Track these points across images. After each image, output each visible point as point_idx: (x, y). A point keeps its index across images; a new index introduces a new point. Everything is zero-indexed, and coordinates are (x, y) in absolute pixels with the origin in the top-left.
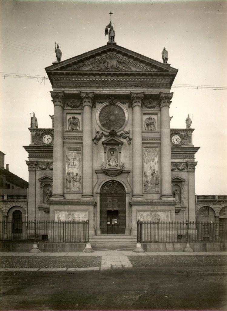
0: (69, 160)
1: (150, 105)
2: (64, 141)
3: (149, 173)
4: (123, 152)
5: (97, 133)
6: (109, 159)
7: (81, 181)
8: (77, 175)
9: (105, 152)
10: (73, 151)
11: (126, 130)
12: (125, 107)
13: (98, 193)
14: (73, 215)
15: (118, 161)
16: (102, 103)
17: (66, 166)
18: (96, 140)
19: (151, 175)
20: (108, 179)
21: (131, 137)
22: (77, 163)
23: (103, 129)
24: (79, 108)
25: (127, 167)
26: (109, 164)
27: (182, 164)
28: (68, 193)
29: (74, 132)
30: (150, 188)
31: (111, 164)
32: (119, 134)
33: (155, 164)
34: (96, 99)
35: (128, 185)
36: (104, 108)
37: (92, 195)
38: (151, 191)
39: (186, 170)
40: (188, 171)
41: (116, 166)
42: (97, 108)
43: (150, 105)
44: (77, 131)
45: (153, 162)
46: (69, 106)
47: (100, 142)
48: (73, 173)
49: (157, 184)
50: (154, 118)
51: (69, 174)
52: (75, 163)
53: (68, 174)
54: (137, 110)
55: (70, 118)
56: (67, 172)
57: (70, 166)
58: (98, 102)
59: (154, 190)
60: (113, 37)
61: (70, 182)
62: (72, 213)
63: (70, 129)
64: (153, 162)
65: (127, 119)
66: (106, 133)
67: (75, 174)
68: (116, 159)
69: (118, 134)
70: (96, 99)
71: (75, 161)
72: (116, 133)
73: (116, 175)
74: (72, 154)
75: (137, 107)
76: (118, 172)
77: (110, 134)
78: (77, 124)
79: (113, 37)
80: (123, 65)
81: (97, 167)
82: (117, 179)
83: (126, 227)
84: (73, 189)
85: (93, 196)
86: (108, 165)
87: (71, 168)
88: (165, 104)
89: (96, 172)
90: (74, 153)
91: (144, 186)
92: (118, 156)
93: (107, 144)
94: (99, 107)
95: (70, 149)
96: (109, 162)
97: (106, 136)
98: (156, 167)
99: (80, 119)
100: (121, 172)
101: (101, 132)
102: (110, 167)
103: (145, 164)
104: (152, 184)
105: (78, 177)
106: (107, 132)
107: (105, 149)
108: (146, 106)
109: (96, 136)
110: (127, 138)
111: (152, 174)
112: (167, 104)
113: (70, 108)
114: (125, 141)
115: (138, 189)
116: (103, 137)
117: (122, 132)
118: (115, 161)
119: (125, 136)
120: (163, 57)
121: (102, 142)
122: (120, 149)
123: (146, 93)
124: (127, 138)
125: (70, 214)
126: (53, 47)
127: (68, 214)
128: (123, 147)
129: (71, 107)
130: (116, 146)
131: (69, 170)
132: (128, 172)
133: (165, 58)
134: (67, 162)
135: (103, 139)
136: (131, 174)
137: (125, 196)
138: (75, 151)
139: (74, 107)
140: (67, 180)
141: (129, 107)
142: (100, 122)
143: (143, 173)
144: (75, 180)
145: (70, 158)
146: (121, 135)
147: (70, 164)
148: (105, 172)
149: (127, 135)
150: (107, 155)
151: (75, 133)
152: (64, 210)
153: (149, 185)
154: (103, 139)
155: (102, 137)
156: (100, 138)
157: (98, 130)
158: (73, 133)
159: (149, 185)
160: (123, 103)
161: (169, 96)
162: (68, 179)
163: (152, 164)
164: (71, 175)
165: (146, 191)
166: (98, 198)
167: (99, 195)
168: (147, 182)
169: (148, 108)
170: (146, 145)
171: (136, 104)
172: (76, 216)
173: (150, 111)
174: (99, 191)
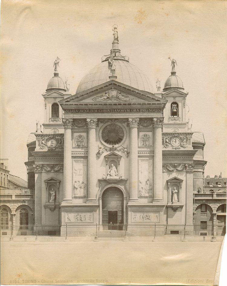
1: (145, 125)
9: (107, 164)
10: (79, 164)
18: (98, 154)
24: (85, 128)
27: (181, 165)
28: (75, 198)
39: (184, 170)
40: (186, 172)
42: (99, 127)
43: (145, 125)
47: (102, 157)
86: (109, 175)
102: (112, 178)
108: (142, 125)
109: (99, 151)
115: (135, 195)
121: (104, 156)
123: (142, 117)
135: (106, 153)
136: (128, 182)
140: (74, 187)
143: (139, 181)
164: (77, 182)
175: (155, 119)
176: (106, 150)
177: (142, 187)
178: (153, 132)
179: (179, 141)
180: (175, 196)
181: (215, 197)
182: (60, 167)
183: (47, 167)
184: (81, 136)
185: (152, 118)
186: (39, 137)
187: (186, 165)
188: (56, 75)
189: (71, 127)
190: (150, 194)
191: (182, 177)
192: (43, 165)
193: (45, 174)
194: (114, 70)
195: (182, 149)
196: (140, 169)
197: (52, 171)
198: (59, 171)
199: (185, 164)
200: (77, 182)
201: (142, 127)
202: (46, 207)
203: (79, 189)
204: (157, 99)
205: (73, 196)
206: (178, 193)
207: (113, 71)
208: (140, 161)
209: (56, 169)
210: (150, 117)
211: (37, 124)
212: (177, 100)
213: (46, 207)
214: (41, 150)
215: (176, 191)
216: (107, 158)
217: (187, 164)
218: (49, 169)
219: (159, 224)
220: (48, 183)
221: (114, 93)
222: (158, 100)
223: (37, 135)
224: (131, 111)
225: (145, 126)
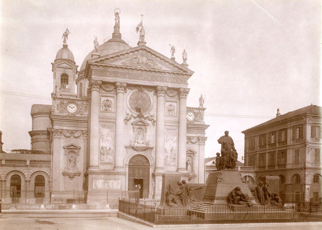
0: (103, 136)
1: (171, 95)
3: (169, 151)
4: (148, 130)
5: (128, 114)
6: (137, 137)
7: (113, 154)
8: (110, 149)
10: (106, 129)
11: (152, 114)
12: (151, 94)
14: (108, 183)
16: (132, 90)
17: (101, 141)
18: (127, 120)
19: (170, 151)
20: (136, 153)
21: (155, 119)
22: (110, 139)
23: (133, 111)
25: (152, 145)
28: (102, 164)
29: (107, 112)
30: (169, 162)
31: (139, 141)
32: (145, 116)
33: (174, 142)
34: (129, 86)
35: (152, 158)
36: (134, 93)
38: (170, 164)
42: (127, 94)
43: (171, 95)
44: (110, 112)
45: (172, 140)
46: (104, 90)
48: (106, 148)
50: (174, 106)
51: (102, 148)
52: (108, 139)
53: (102, 148)
54: (161, 99)
55: (105, 100)
56: (101, 147)
57: (104, 141)
58: (128, 88)
59: (173, 163)
60: (143, 36)
61: (104, 155)
62: (107, 181)
63: (104, 109)
64: (172, 140)
65: (152, 104)
66: (135, 115)
67: (108, 148)
68: (143, 137)
69: (145, 116)
70: (129, 86)
71: (108, 138)
72: (143, 116)
73: (143, 151)
74: (105, 131)
75: (161, 97)
77: (138, 116)
78: (111, 107)
79: (143, 36)
80: (151, 61)
81: (128, 144)
83: (149, 193)
84: (106, 161)
86: (136, 143)
87: (105, 143)
88: (183, 96)
89: (126, 148)
90: (107, 130)
92: (145, 134)
93: (136, 125)
94: (130, 92)
95: (104, 126)
97: (135, 118)
98: (175, 145)
99: (113, 101)
100: (146, 149)
101: (130, 114)
102: (139, 145)
103: (166, 142)
104: (171, 159)
105: (110, 151)
106: (136, 114)
107: (134, 128)
110: (152, 120)
111: (171, 151)
112: (186, 96)
113: (104, 92)
114: (149, 122)
116: (132, 118)
117: (148, 115)
119: (150, 118)
120: (183, 57)
122: (146, 129)
124: (152, 120)
125: (106, 182)
126: (94, 39)
127: (104, 183)
128: (148, 127)
129: (106, 91)
130: (143, 127)
131: (104, 144)
132: (152, 148)
134: (101, 138)
135: (133, 120)
137: (149, 168)
138: (108, 129)
139: (108, 91)
140: (101, 153)
141: (154, 95)
142: (130, 105)
144: (108, 153)
145: (104, 134)
146: (147, 117)
147: (104, 140)
148: (133, 148)
149: (152, 118)
150: (135, 133)
151: (108, 114)
152: (101, 179)
153: (169, 159)
154: (133, 120)
155: (131, 118)
156: (130, 119)
157: (128, 112)
158: (106, 114)
159: (169, 159)
160: (149, 91)
161: (187, 90)
162: (103, 152)
163: (171, 142)
165: (166, 164)
166: (127, 169)
167: (128, 166)
168: (167, 157)
169: (169, 97)
170: (166, 127)
171: (161, 94)
172: (110, 184)
173: (171, 99)
174: (128, 163)
176: (134, 117)
178: (178, 102)
181: (276, 168)
182: (80, 134)
183: (67, 133)
184: (109, 101)
188: (65, 47)
193: (64, 139)
195: (196, 123)
197: (72, 137)
198: (79, 138)
201: (168, 97)
202: (64, 174)
204: (184, 70)
205: (100, 162)
209: (76, 135)
210: (177, 87)
213: (64, 174)
214: (61, 114)
218: (68, 135)
220: (67, 148)
222: (185, 71)
225: (171, 97)
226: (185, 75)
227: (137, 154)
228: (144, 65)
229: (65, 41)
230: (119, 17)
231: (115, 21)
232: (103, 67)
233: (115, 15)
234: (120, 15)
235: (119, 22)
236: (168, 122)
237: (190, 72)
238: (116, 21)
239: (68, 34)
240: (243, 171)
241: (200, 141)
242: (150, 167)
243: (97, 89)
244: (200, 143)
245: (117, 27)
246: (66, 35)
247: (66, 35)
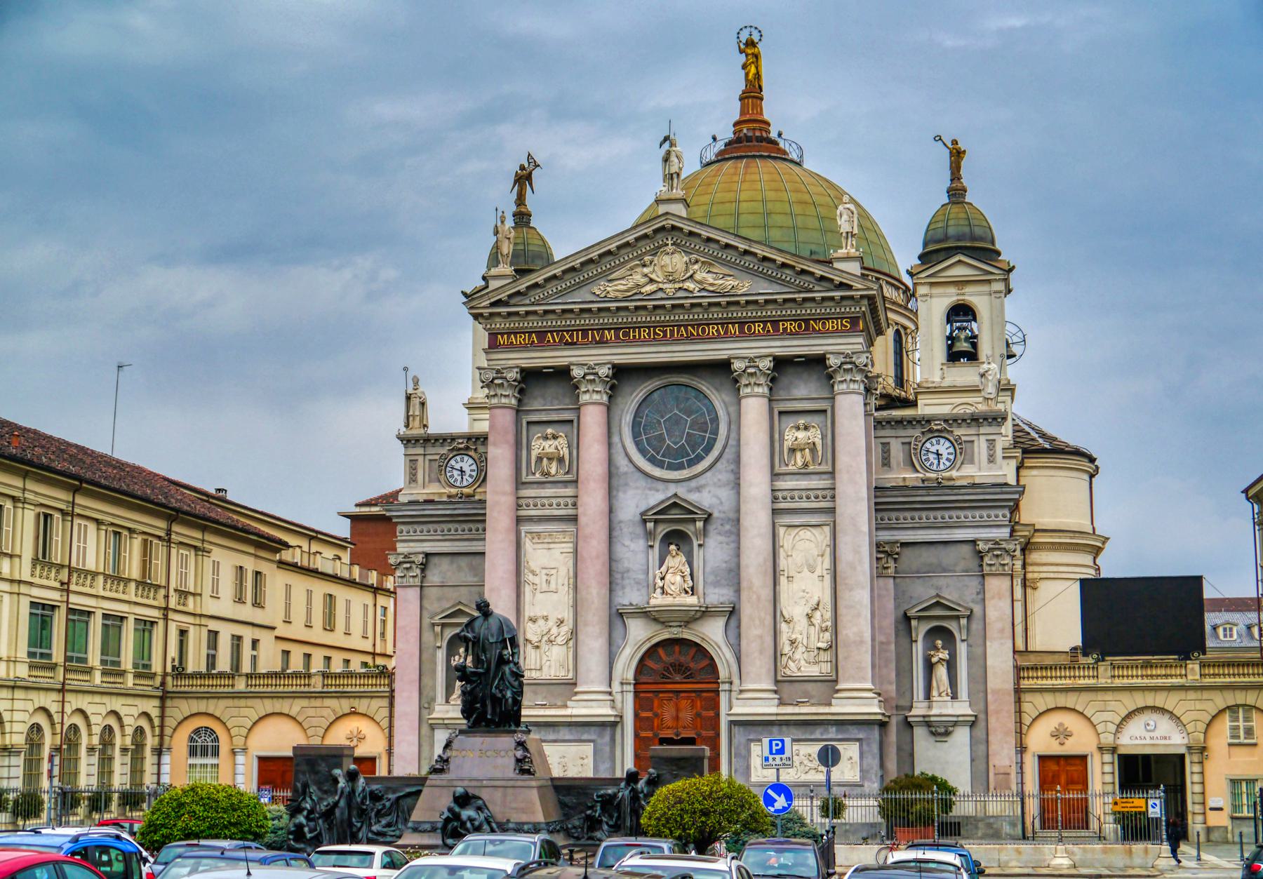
2: (522, 513)
13: (627, 684)
15: (692, 575)
19: (805, 621)
26: (663, 588)
37: (609, 690)
41: (687, 592)
49: (825, 650)
61: (537, 647)
75: (754, 399)
76: (693, 613)
82: (686, 634)
85: (610, 694)
91: (782, 655)
96: (662, 579)
102: (668, 600)
111: (809, 617)
118: (683, 577)
133: (847, 233)
137: (717, 692)
147: (538, 587)
159: (801, 649)
164: (541, 622)
165: (789, 673)
166: (630, 698)
167: (631, 688)
174: (630, 676)
175: (833, 361)
177: (794, 637)
179: (951, 450)
180: (941, 672)
185: (824, 355)
186: (414, 446)
187: (981, 546)
189: (514, 402)
190: (826, 668)
191: (956, 591)
192: (427, 555)
194: (675, 176)
196: (782, 563)
199: (974, 542)
200: (541, 622)
203: (544, 647)
204: (837, 279)
206: (951, 665)
207: (672, 179)
208: (782, 531)
211: (408, 398)
212: (977, 298)
215: (944, 655)
216: (650, 521)
217: (987, 541)
219: (858, 790)
221: (674, 261)
222: (842, 286)
223: (409, 441)
224: (744, 329)
226: (843, 298)
227: (666, 636)
228: (677, 286)
229: (520, 200)
230: (757, 56)
231: (743, 73)
232: (504, 317)
233: (741, 52)
234: (761, 47)
235: (758, 76)
236: (817, 497)
237: (860, 286)
238: (747, 75)
239: (530, 174)
240: (1208, 681)
241: (987, 560)
242: (723, 687)
243: (504, 400)
244: (986, 569)
245: (752, 93)
246: (523, 179)
247: (523, 179)
